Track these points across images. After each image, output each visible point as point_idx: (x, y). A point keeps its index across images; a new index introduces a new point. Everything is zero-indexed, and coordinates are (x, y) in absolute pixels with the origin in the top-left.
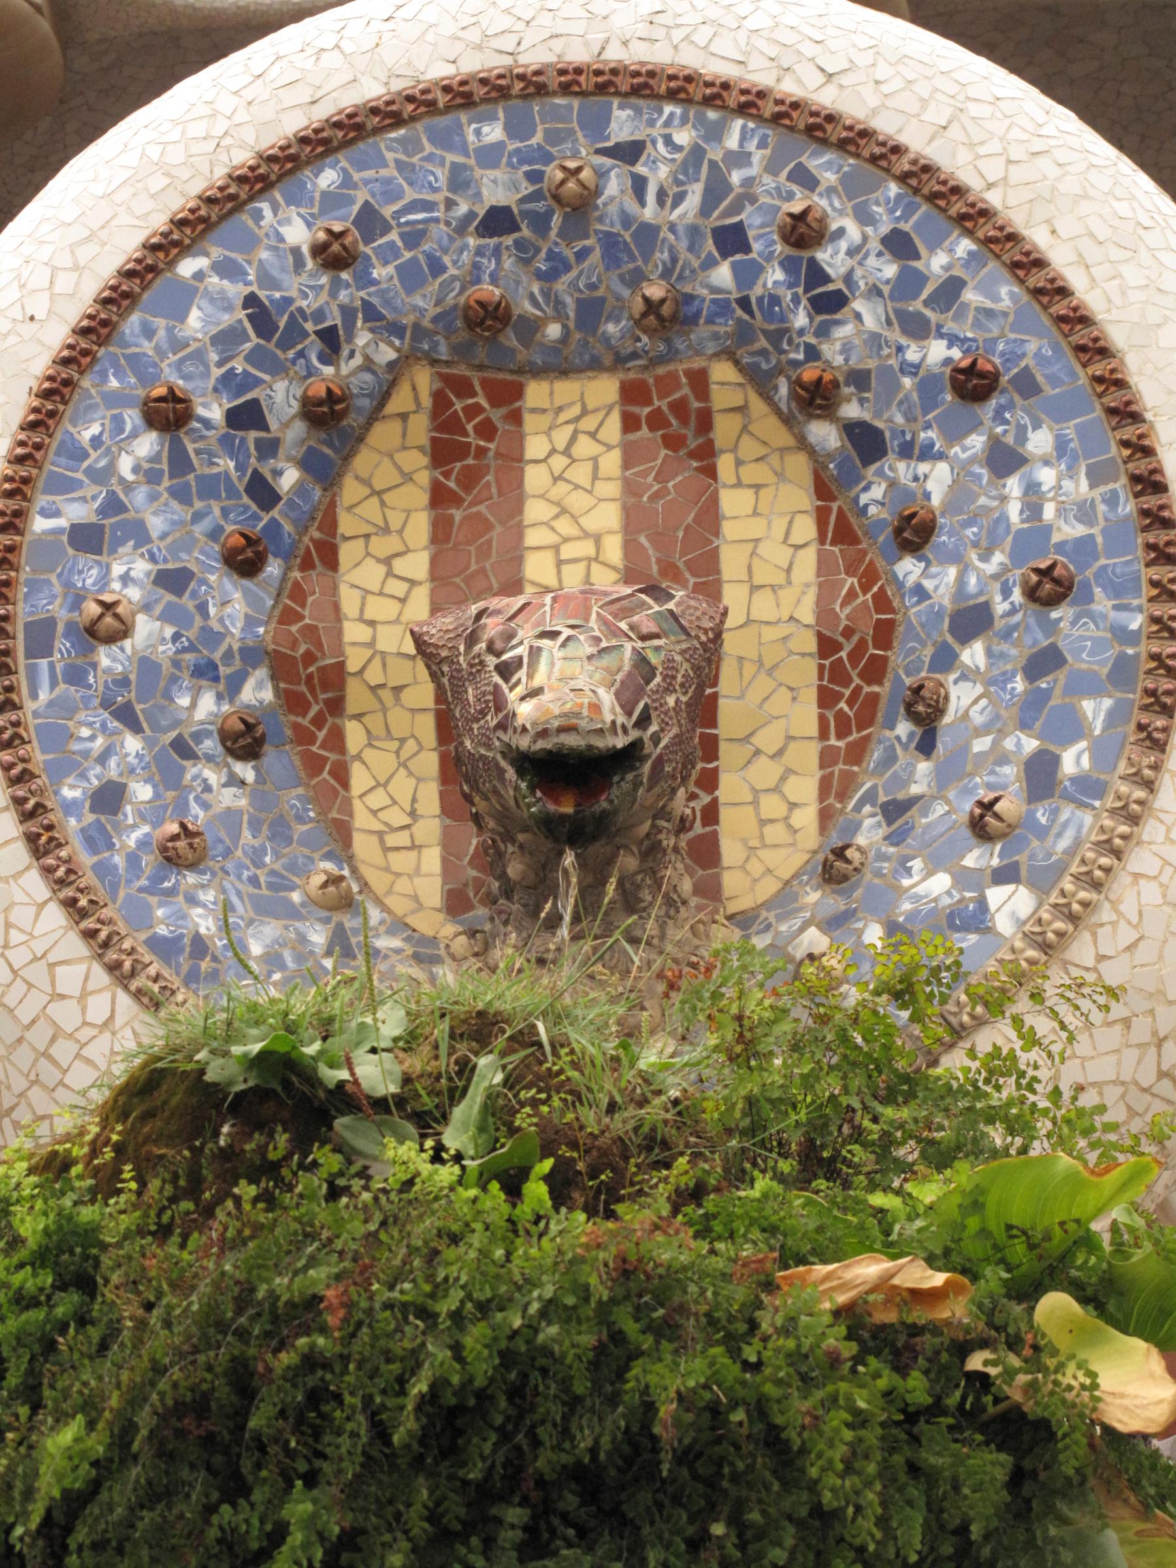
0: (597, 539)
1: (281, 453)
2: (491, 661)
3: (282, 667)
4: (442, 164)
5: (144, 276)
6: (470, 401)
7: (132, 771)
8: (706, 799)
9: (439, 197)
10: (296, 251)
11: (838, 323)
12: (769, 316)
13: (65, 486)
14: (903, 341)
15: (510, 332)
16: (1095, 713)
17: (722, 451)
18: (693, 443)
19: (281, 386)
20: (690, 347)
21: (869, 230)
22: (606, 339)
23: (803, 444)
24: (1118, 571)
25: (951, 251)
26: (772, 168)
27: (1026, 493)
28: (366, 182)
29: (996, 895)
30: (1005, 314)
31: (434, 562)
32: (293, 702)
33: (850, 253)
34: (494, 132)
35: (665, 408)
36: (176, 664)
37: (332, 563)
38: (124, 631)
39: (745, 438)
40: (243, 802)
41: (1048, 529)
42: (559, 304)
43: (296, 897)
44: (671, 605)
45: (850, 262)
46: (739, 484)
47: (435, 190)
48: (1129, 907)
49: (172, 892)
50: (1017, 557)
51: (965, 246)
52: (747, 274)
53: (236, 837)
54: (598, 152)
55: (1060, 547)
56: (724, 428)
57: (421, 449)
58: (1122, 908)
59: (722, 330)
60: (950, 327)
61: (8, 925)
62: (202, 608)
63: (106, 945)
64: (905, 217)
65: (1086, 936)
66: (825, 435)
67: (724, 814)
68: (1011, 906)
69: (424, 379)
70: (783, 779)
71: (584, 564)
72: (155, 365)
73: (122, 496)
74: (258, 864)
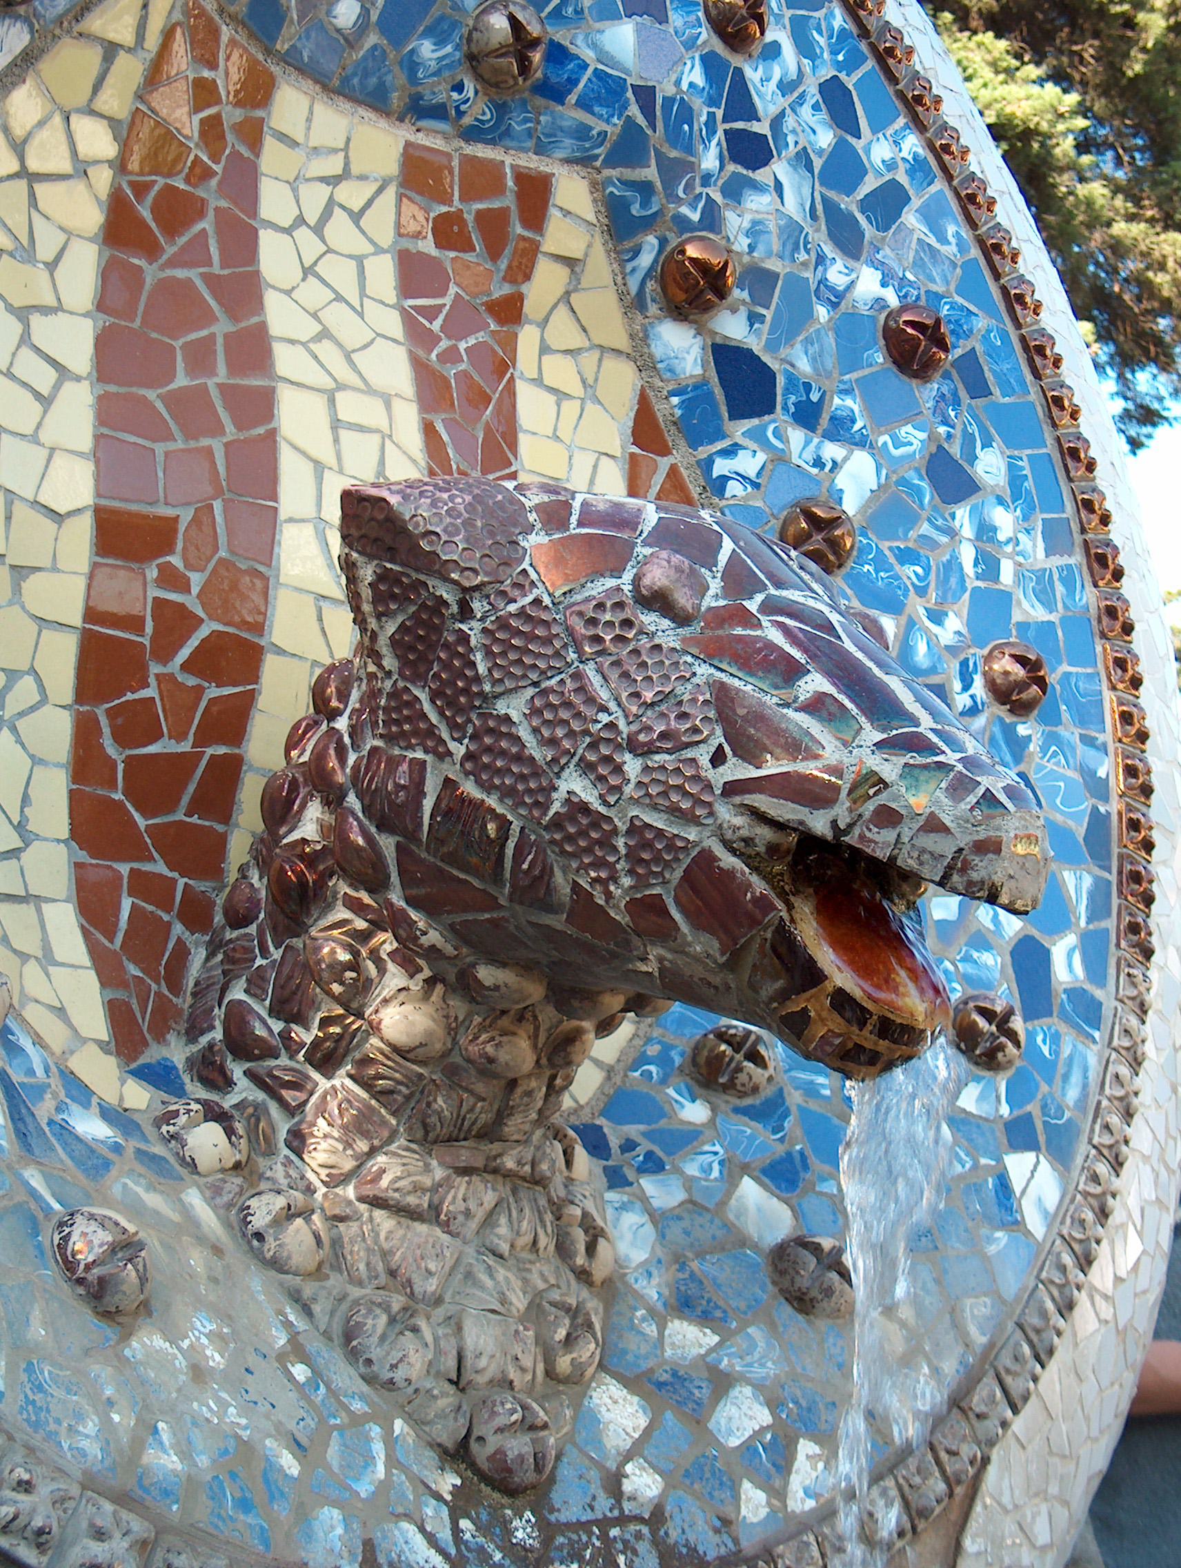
6: (206, 74)
11: (757, 187)
12: (674, 136)
14: (829, 250)
16: (1078, 889)
18: (501, 290)
20: (530, 133)
22: (411, 64)
23: (641, 355)
27: (979, 537)
29: (1019, 1165)
31: (103, 343)
35: (469, 218)
39: (561, 316)
45: (783, 102)
46: (538, 382)
51: (912, 144)
56: (545, 282)
57: (113, 122)
59: (598, 126)
66: (682, 348)
71: (376, 438)
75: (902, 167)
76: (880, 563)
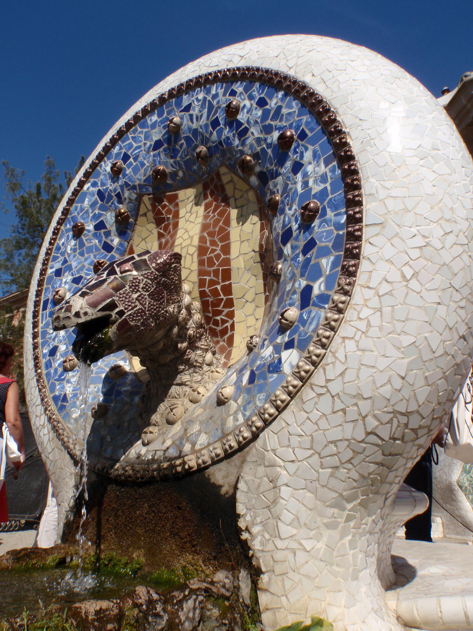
0: (192, 238)
1: (112, 234)
7: (61, 342)
8: (231, 322)
9: (142, 144)
13: (55, 258)
14: (266, 136)
17: (230, 197)
21: (252, 102)
22: (195, 171)
24: (336, 199)
25: (277, 97)
26: (224, 95)
27: (303, 178)
28: (124, 146)
29: (285, 354)
30: (295, 112)
33: (247, 113)
34: (155, 118)
39: (236, 191)
41: (311, 189)
42: (180, 165)
47: (141, 141)
48: (340, 355)
54: (181, 112)
55: (315, 196)
56: (229, 190)
58: (337, 355)
64: (262, 92)
65: (320, 370)
68: (291, 358)
70: (255, 310)
72: (77, 218)
73: (67, 258)
75: (279, 101)
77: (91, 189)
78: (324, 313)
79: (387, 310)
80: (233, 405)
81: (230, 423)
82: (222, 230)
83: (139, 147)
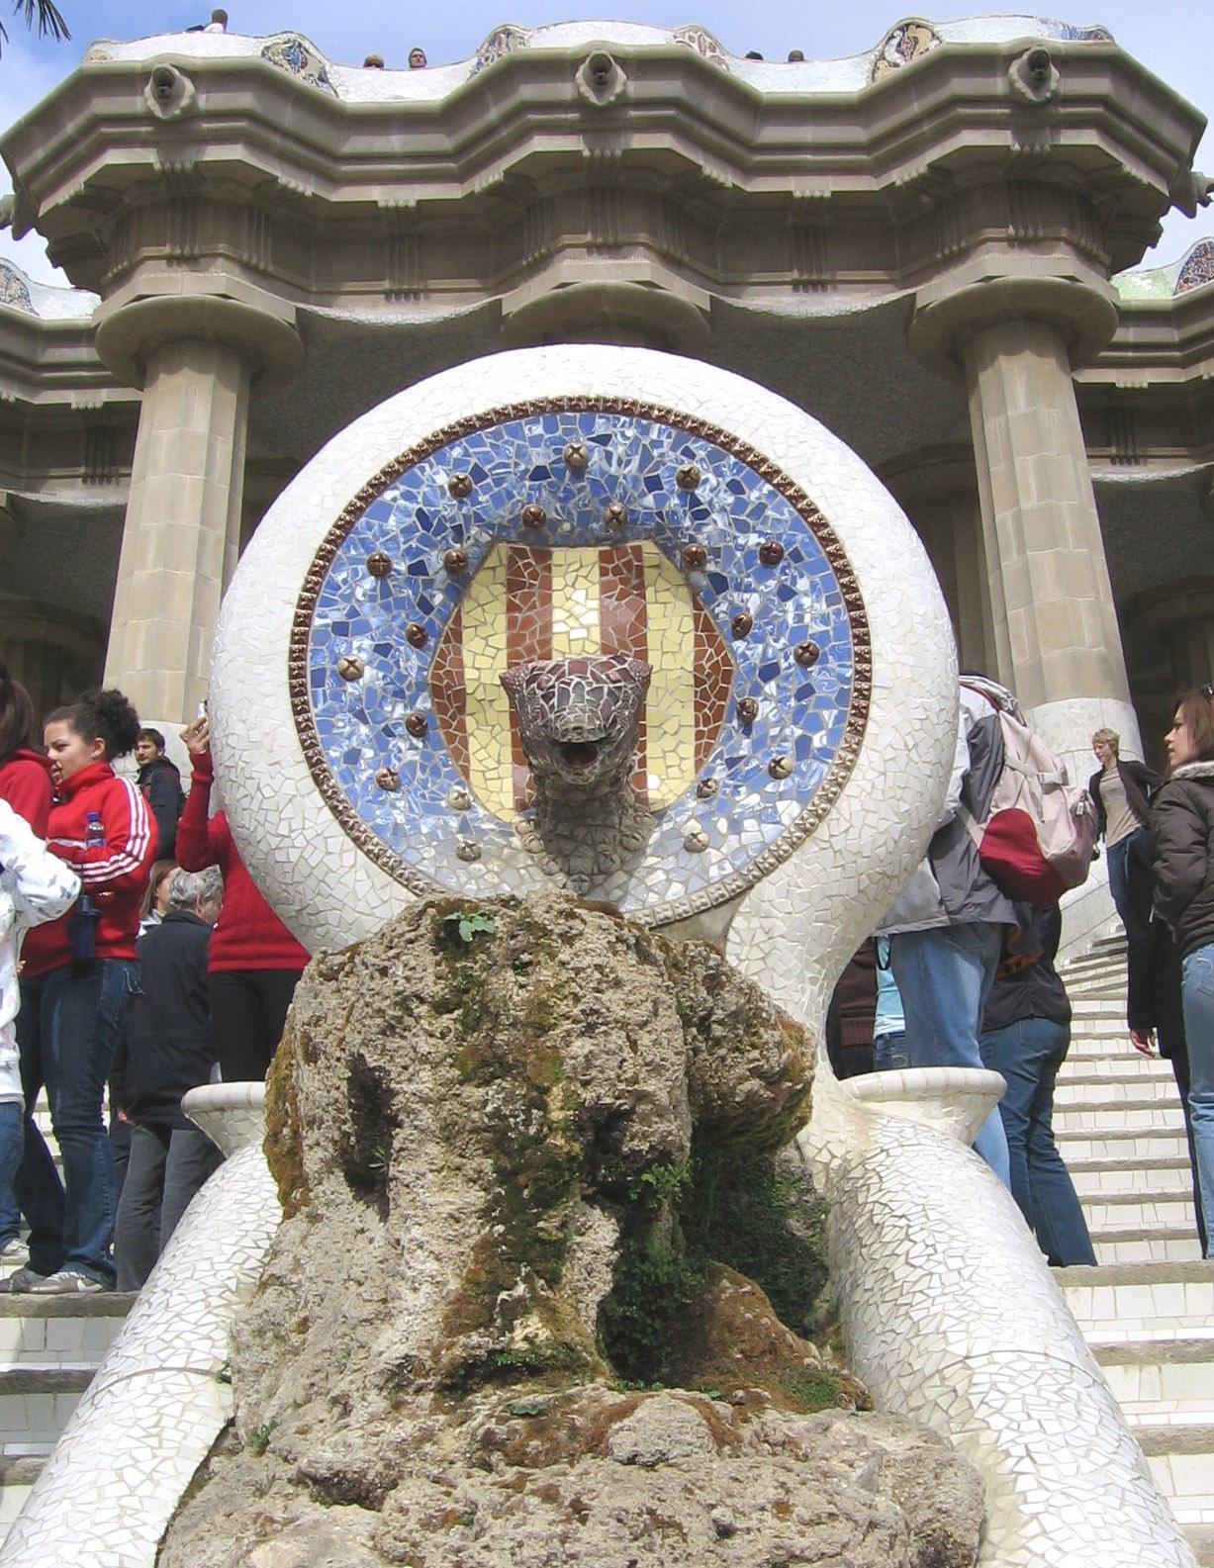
2: (540, 693)
3: (436, 692)
4: (512, 444)
5: (368, 498)
8: (640, 755)
10: (441, 487)
15: (546, 528)
18: (635, 582)
19: (434, 553)
22: (592, 530)
23: (688, 584)
26: (673, 448)
29: (781, 805)
32: (442, 709)
33: (712, 491)
34: (538, 430)
36: (384, 690)
37: (459, 639)
38: (359, 674)
40: (417, 758)
41: (807, 627)
42: (570, 514)
43: (443, 804)
44: (626, 666)
49: (382, 803)
50: (791, 641)
51: (768, 488)
52: (661, 500)
53: (414, 775)
55: (812, 636)
56: (649, 575)
60: (760, 527)
61: (304, 818)
62: (397, 663)
63: (352, 828)
64: (738, 473)
67: (649, 762)
69: (503, 549)
74: (425, 788)
76: (760, 628)
77: (402, 502)
78: (825, 770)
79: (890, 775)
80: (713, 855)
81: (714, 872)
82: (634, 629)
83: (506, 466)
